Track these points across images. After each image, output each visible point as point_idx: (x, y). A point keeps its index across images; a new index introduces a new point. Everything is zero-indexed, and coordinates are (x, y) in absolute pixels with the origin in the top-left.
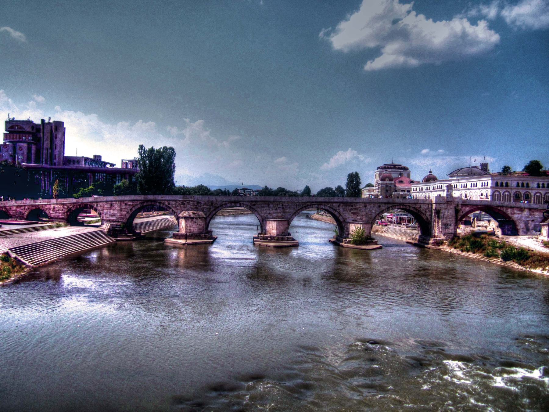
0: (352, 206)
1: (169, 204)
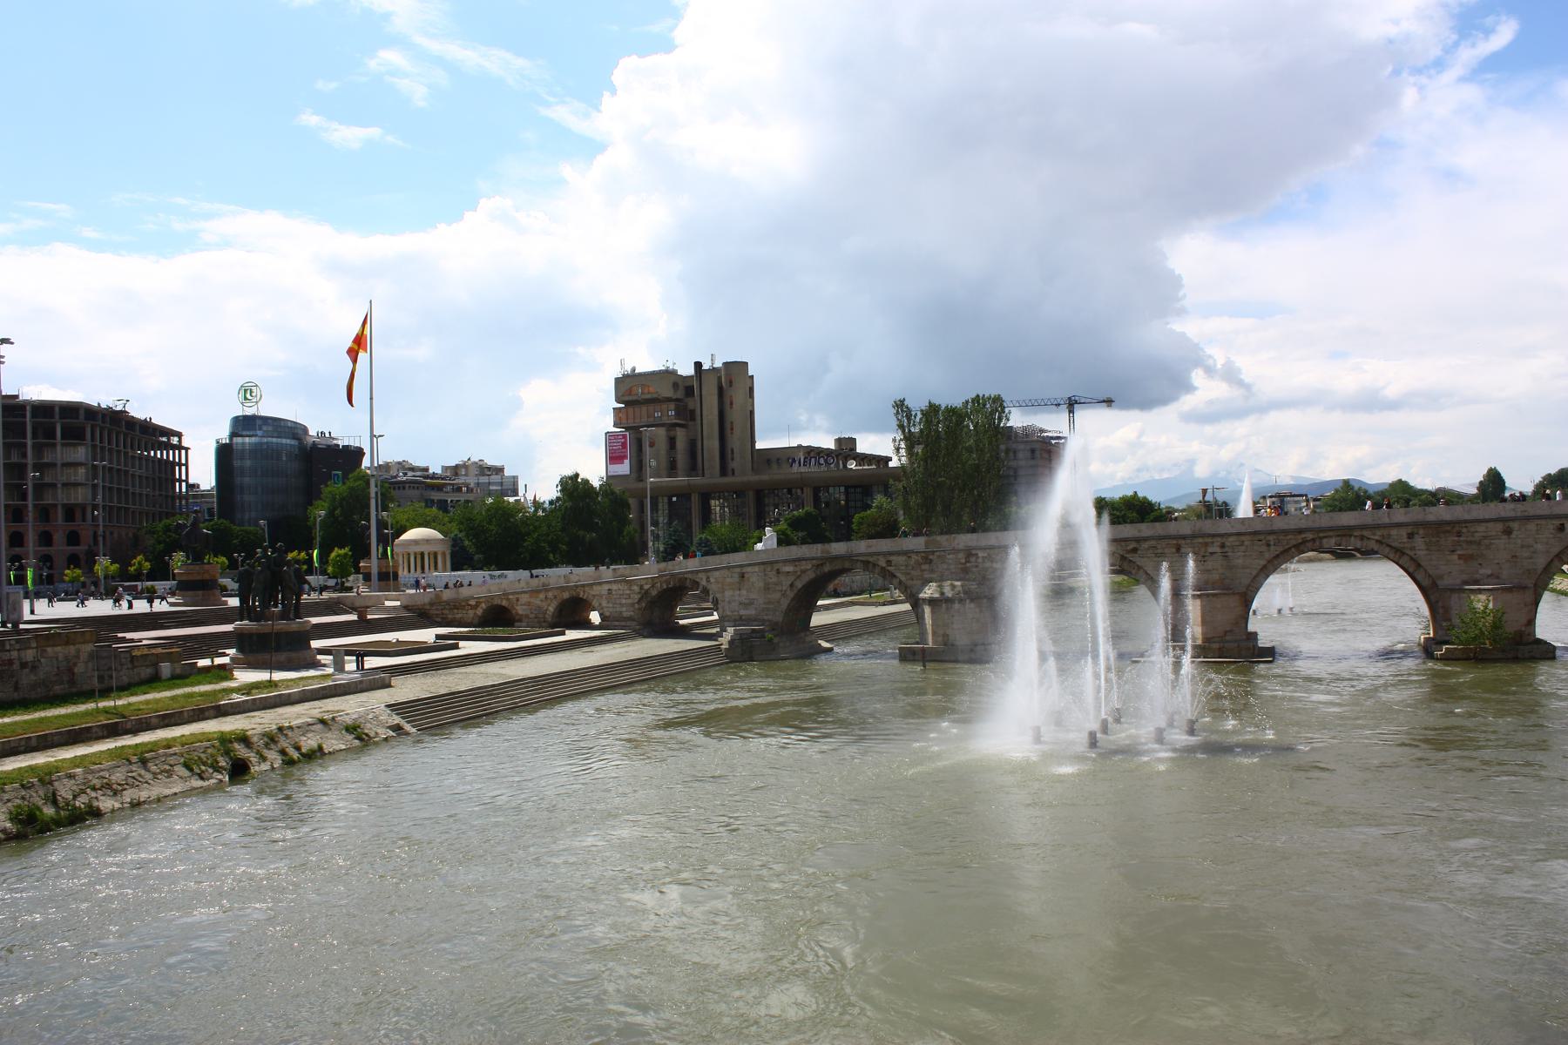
0: (1459, 534)
1: (889, 563)
